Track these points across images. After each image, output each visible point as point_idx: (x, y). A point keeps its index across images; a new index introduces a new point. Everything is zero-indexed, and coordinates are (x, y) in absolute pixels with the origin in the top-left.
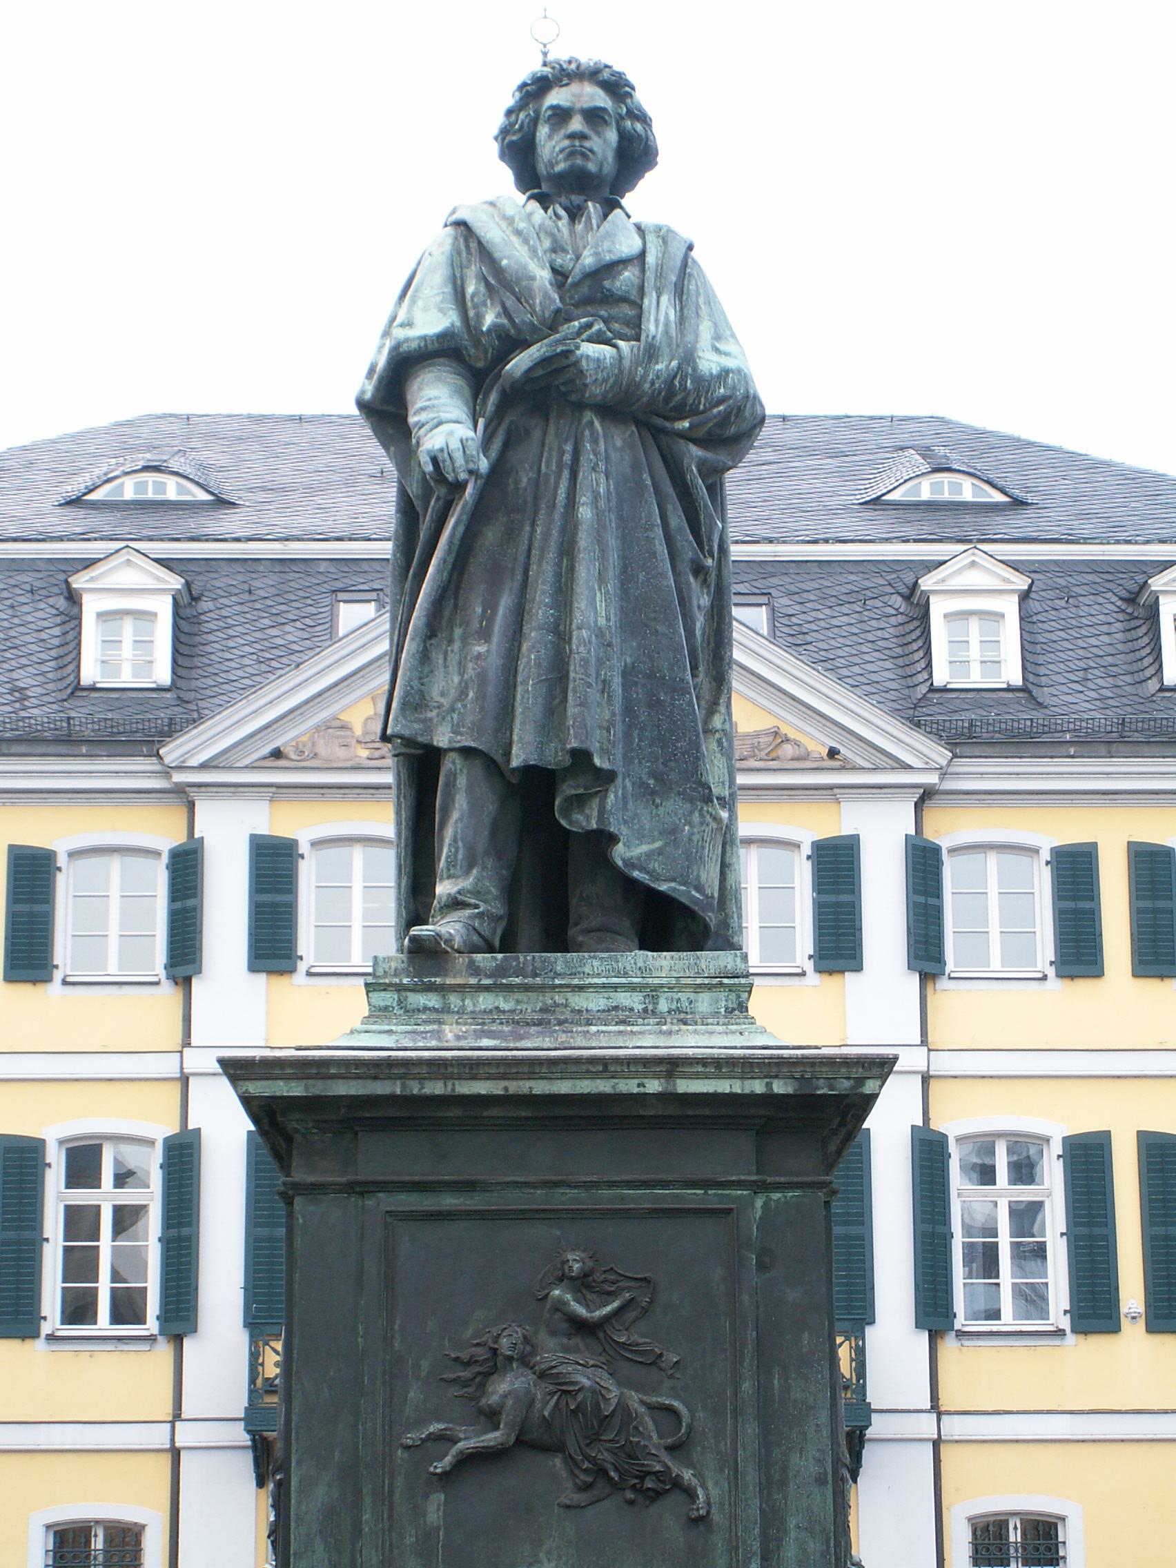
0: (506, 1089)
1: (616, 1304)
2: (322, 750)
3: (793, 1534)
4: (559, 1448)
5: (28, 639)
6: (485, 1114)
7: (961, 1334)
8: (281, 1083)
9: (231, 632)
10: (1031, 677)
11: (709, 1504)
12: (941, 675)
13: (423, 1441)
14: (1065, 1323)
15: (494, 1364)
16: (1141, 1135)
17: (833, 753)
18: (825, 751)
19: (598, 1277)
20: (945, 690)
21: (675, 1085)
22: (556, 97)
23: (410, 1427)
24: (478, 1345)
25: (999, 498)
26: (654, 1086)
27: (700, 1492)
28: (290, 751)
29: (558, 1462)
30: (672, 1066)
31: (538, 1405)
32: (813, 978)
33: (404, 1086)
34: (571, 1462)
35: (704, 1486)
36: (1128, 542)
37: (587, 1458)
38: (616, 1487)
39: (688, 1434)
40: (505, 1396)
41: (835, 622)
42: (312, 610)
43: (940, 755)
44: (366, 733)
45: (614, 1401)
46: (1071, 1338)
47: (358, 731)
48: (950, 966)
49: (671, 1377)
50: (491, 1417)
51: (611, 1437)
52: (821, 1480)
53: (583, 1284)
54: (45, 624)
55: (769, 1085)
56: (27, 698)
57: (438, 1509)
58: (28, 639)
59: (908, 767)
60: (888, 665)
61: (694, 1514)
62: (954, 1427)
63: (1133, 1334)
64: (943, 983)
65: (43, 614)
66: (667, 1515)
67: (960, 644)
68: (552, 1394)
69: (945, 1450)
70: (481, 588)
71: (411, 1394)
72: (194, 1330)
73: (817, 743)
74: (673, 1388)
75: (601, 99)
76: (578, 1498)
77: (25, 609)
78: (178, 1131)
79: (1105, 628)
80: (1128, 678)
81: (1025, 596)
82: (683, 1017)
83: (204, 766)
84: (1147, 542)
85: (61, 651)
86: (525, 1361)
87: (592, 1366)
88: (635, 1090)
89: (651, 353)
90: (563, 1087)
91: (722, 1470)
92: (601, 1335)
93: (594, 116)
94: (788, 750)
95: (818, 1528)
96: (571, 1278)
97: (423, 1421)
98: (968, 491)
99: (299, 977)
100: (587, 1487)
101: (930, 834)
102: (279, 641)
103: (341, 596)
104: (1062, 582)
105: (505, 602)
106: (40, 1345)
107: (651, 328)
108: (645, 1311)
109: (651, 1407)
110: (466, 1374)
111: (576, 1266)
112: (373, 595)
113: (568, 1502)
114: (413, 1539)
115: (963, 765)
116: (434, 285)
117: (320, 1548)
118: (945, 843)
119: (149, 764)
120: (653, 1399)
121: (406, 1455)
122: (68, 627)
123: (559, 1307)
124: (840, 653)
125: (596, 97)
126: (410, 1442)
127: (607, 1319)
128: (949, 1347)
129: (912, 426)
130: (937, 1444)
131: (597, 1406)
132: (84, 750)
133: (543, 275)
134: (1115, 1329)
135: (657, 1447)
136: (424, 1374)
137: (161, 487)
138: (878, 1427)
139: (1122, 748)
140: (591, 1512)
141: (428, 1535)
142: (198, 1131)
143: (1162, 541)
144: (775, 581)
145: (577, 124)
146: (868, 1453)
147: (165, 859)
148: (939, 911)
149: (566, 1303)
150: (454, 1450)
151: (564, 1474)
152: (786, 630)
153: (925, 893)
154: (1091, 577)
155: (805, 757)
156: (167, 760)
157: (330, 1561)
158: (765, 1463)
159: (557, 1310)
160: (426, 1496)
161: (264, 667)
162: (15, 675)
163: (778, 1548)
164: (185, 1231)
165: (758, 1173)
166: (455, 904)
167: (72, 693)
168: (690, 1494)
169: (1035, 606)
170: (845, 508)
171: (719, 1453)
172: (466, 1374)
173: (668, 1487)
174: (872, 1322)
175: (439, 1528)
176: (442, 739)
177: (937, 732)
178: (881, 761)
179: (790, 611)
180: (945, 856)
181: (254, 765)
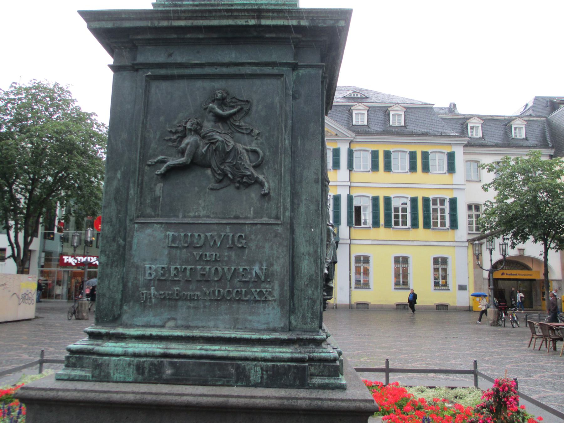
0: (192, 23)
1: (235, 110)
3: (304, 202)
4: (209, 166)
6: (186, 37)
7: (354, 227)
8: (104, 22)
11: (269, 189)
12: (354, 123)
13: (156, 163)
16: (384, 197)
17: (336, 135)
19: (228, 100)
20: (355, 125)
21: (260, 22)
23: (151, 157)
24: (180, 126)
25: (364, 97)
26: (252, 22)
27: (266, 184)
29: (209, 172)
31: (201, 148)
33: (152, 23)
34: (214, 171)
35: (268, 182)
37: (219, 168)
38: (232, 181)
39: (262, 161)
40: (187, 144)
43: (354, 135)
45: (231, 147)
48: (354, 169)
49: (256, 139)
50: (182, 153)
51: (230, 161)
52: (316, 181)
53: (222, 102)
55: (299, 22)
57: (160, 189)
59: (348, 137)
61: (263, 192)
62: (354, 242)
64: (353, 172)
66: (253, 194)
67: (357, 118)
68: (207, 144)
69: (351, 245)
71: (152, 145)
74: (257, 144)
76: (216, 186)
81: (368, 111)
86: (197, 132)
87: (224, 133)
88: (244, 23)
90: (215, 23)
91: (275, 176)
92: (228, 122)
94: (329, 134)
95: (314, 200)
96: (217, 99)
97: (155, 156)
100: (220, 181)
101: (351, 148)
108: (247, 113)
109: (247, 151)
110: (175, 137)
111: (219, 95)
113: (212, 187)
114: (149, 201)
115: (358, 137)
117: (113, 204)
118: (354, 150)
120: (248, 148)
121: (148, 168)
123: (211, 111)
126: (150, 163)
127: (231, 115)
128: (352, 229)
130: (350, 244)
131: (224, 149)
135: (249, 166)
136: (157, 137)
138: (340, 241)
140: (221, 191)
141: (156, 199)
146: (339, 245)
148: (353, 160)
149: (214, 109)
150: (165, 165)
151: (211, 177)
155: (332, 135)
157: (117, 209)
158: (293, 173)
159: (210, 112)
160: (155, 185)
163: (298, 208)
165: (294, 60)
168: (262, 185)
169: (369, 113)
170: (339, 98)
171: (275, 169)
172: (175, 137)
173: (253, 182)
174: (340, 225)
175: (160, 197)
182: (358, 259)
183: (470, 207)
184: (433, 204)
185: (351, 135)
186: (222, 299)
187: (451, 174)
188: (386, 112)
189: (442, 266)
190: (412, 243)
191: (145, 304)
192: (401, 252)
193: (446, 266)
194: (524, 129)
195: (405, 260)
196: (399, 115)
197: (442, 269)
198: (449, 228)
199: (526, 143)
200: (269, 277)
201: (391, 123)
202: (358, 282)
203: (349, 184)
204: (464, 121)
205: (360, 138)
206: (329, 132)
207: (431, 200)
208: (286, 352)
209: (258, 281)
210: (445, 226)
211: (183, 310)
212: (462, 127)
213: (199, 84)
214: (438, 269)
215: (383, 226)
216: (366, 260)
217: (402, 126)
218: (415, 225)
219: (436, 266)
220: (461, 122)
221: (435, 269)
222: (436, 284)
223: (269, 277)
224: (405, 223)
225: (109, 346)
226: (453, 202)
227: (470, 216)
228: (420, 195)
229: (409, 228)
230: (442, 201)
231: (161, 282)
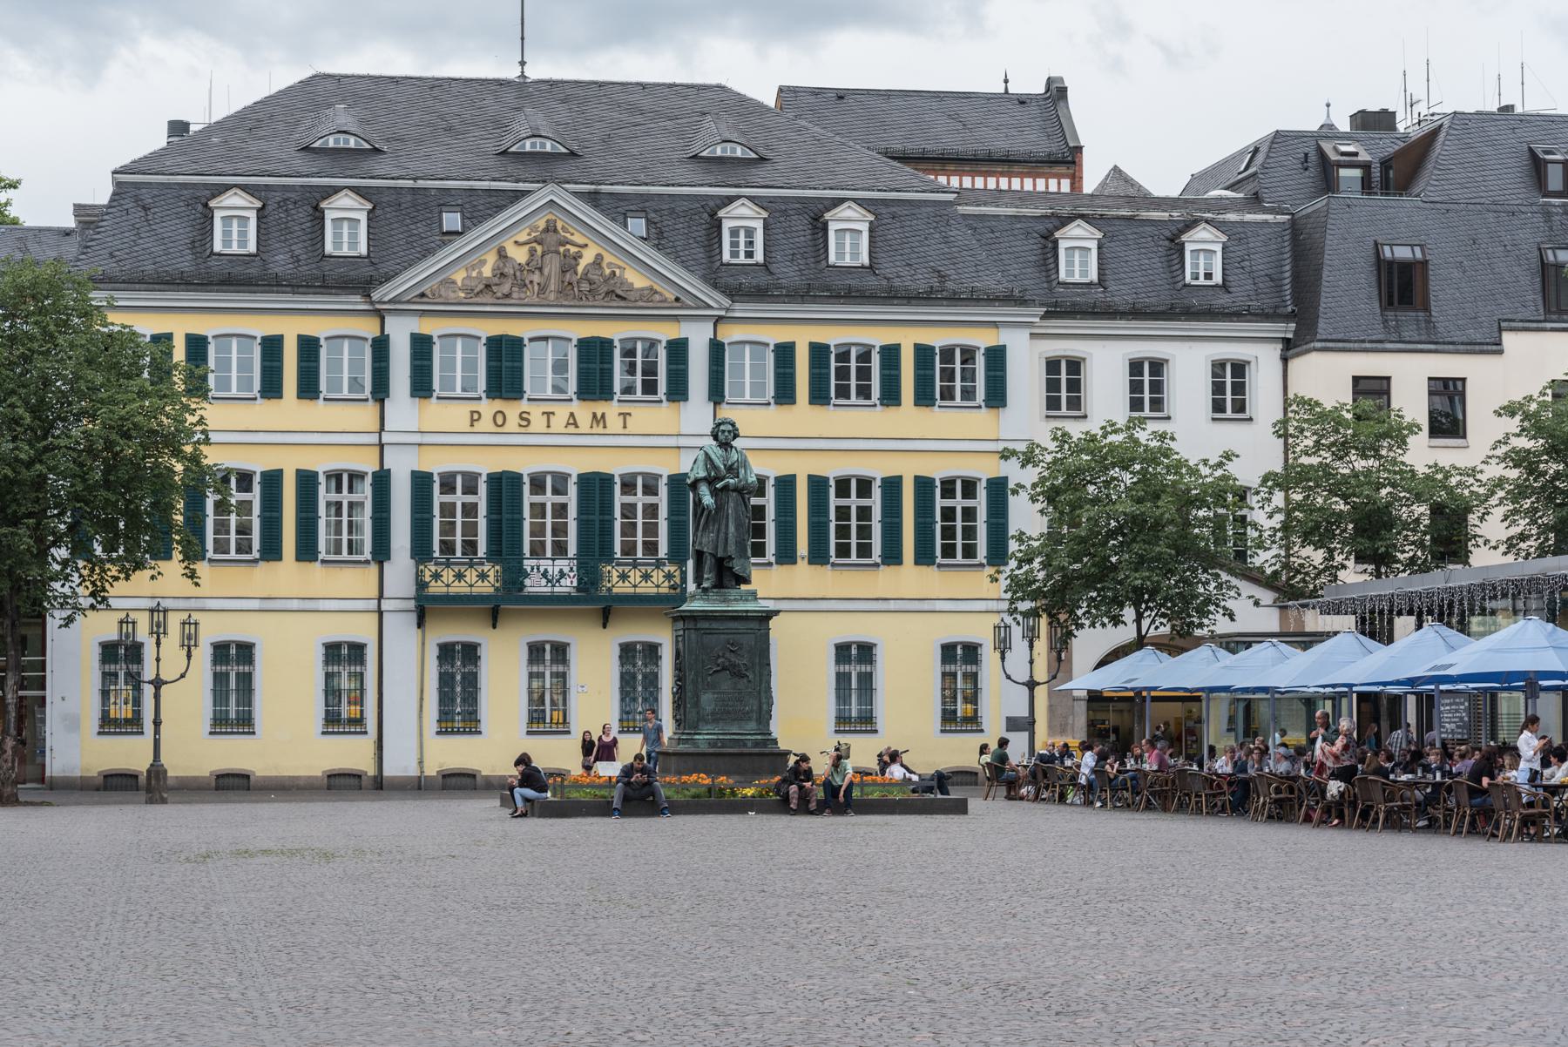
2: (443, 293)
5: (296, 228)
9: (392, 226)
10: (768, 259)
14: (773, 559)
15: (719, 657)
16: (810, 476)
17: (677, 299)
18: (673, 298)
20: (729, 265)
22: (722, 428)
28: (428, 293)
30: (747, 611)
32: (665, 404)
36: (815, 189)
41: (677, 227)
42: (430, 215)
43: (726, 302)
44: (463, 285)
46: (775, 566)
47: (459, 283)
48: (727, 397)
53: (732, 644)
54: (303, 220)
56: (299, 261)
58: (296, 228)
59: (710, 307)
60: (702, 250)
63: (802, 566)
64: (724, 406)
65: (302, 214)
66: (745, 680)
70: (711, 524)
72: (389, 559)
73: (670, 295)
75: (730, 428)
77: (293, 212)
78: (378, 469)
79: (802, 233)
80: (812, 260)
82: (747, 600)
83: (390, 302)
84: (825, 189)
85: (313, 236)
89: (740, 481)
93: (729, 432)
94: (657, 297)
99: (434, 400)
101: (719, 338)
102: (415, 232)
103: (444, 208)
104: (783, 208)
105: (716, 526)
106: (318, 564)
107: (741, 476)
112: (458, 209)
115: (737, 306)
116: (701, 464)
118: (726, 342)
119: (358, 298)
122: (315, 222)
124: (678, 243)
125: (730, 428)
129: (709, 94)
132: (333, 291)
133: (722, 467)
134: (795, 562)
137: (346, 141)
139: (809, 298)
142: (389, 470)
143: (831, 189)
144: (647, 204)
145: (726, 434)
147: (370, 342)
152: (654, 230)
153: (717, 365)
154: (797, 206)
155: (665, 301)
156: (374, 299)
161: (409, 246)
162: (293, 248)
164: (384, 515)
166: (708, 579)
167: (321, 260)
176: (705, 550)
178: (700, 304)
179: (656, 220)
180: (726, 347)
181: (414, 300)
184: (943, 497)
185: (716, 300)
186: (735, 720)
187: (995, 410)
188: (816, 220)
189: (964, 667)
190: (882, 604)
191: (707, 722)
192: (855, 629)
193: (974, 667)
194: (1219, 255)
195: (866, 652)
197: (965, 675)
198: (985, 561)
199: (1223, 300)
200: (752, 711)
201: (832, 259)
204: (1050, 226)
205: (741, 311)
206: (656, 292)
207: (938, 483)
208: (759, 737)
209: (748, 713)
210: (975, 557)
211: (721, 724)
212: (1045, 247)
213: (722, 636)
214: (954, 675)
215: (806, 560)
217: (863, 267)
218: (892, 556)
219: (950, 668)
220: (1040, 227)
221: (944, 674)
222: (949, 717)
223: (752, 711)
224: (865, 551)
225: (697, 737)
226: (998, 489)
228: (908, 470)
229: (876, 565)
230: (969, 487)
231: (712, 714)
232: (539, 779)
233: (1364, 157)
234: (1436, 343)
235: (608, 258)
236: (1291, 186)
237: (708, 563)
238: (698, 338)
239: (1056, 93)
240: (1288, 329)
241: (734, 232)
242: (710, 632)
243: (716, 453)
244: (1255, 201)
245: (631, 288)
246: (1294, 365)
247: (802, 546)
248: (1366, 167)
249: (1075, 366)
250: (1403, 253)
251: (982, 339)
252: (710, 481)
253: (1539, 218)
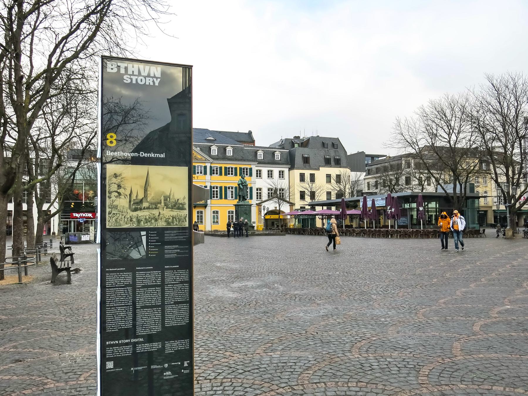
43: (212, 160)
98: (212, 138)
177: (212, 158)
182: (214, 212)
183: (257, 190)
185: (211, 160)
196: (230, 151)
199: (280, 162)
202: (214, 222)
203: (211, 181)
216: (217, 212)
227: (257, 193)
232: (483, 222)
233: (298, 142)
234: (311, 169)
235: (195, 153)
236: (288, 146)
237: (241, 197)
238: (208, 165)
239: (250, 133)
240: (289, 166)
241: (213, 150)
242: (242, 208)
243: (242, 180)
244: (283, 148)
245: (198, 158)
246: (290, 172)
247: (223, 197)
248: (299, 144)
249: (260, 171)
250: (306, 156)
251: (249, 167)
252: (241, 184)
253: (324, 151)
